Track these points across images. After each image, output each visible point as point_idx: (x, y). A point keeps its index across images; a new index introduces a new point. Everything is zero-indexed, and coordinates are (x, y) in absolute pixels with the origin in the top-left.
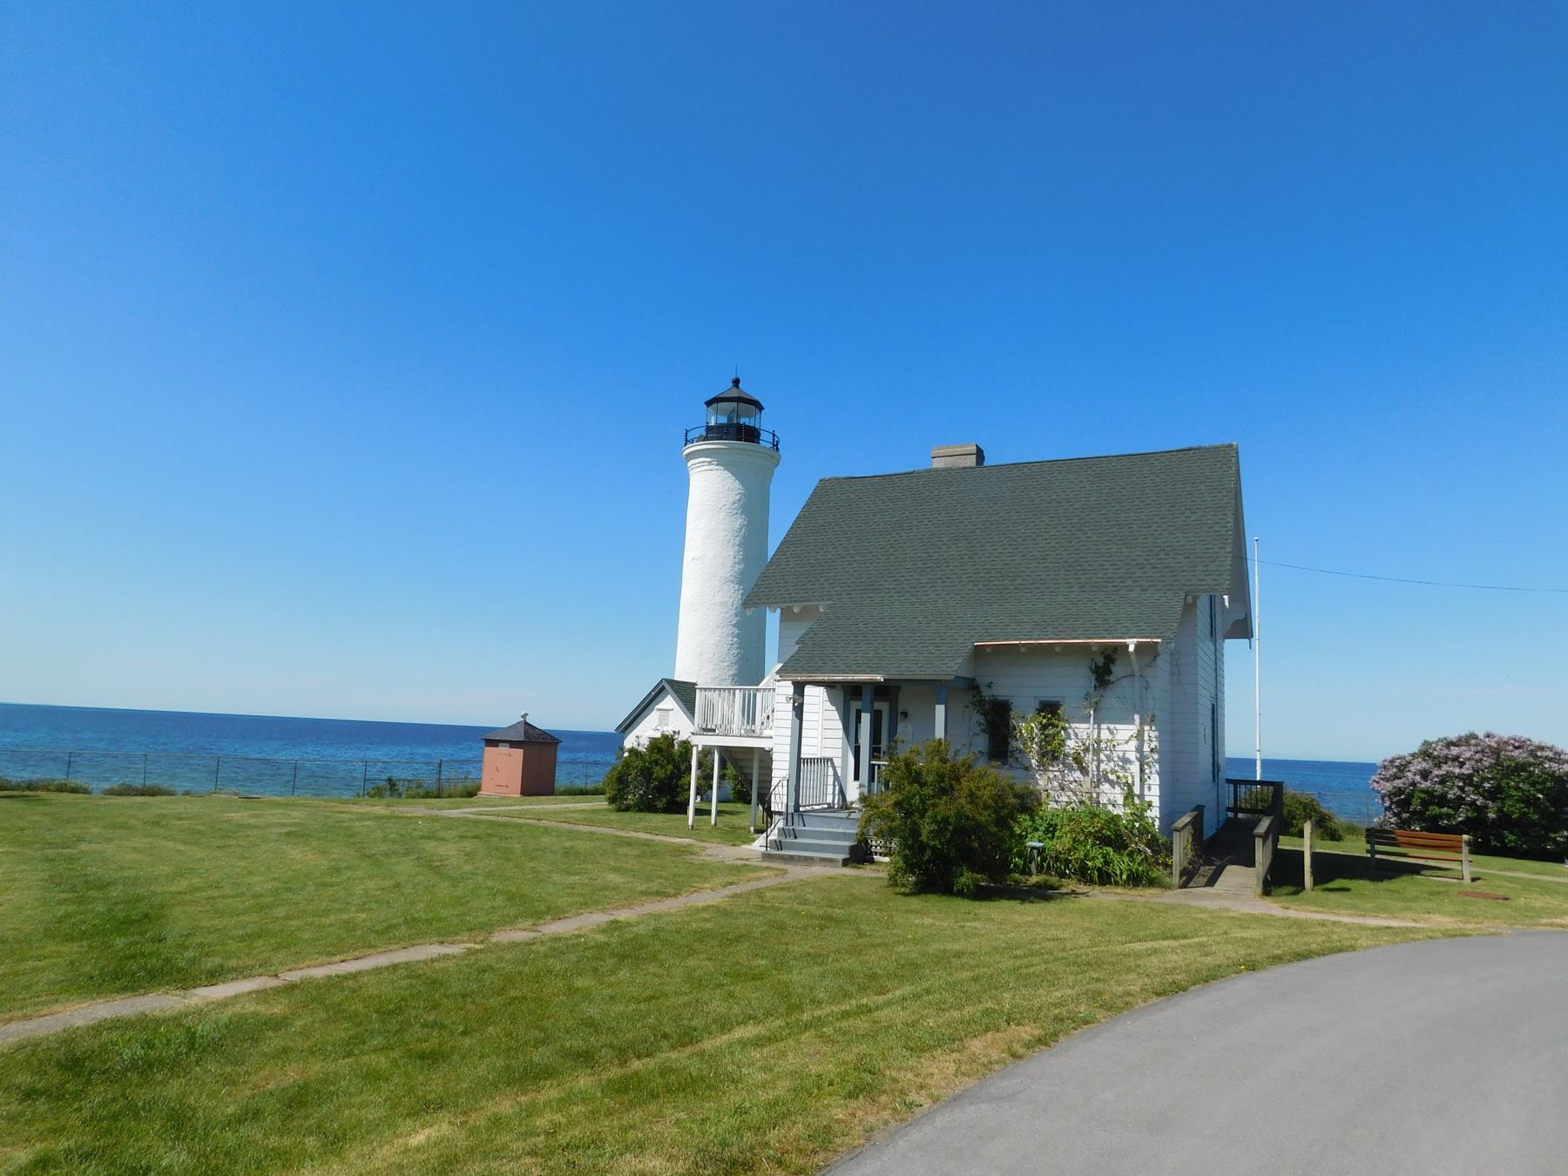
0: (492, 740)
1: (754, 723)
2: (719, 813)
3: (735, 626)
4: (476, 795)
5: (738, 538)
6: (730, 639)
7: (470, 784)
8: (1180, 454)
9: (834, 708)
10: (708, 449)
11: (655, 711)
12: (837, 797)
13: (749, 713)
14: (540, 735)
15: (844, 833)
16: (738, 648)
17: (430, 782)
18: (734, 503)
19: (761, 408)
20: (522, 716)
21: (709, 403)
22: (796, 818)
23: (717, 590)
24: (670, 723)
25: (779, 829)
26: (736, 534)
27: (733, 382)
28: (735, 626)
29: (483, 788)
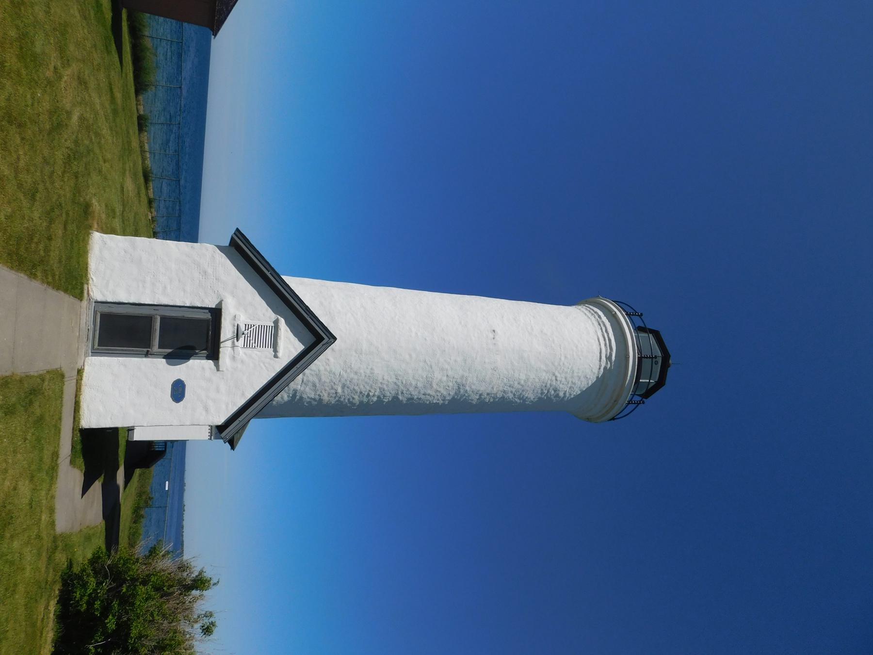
5: (511, 396)
6: (377, 394)
11: (274, 316)
18: (555, 391)
23: (450, 373)
24: (249, 351)
26: (518, 394)
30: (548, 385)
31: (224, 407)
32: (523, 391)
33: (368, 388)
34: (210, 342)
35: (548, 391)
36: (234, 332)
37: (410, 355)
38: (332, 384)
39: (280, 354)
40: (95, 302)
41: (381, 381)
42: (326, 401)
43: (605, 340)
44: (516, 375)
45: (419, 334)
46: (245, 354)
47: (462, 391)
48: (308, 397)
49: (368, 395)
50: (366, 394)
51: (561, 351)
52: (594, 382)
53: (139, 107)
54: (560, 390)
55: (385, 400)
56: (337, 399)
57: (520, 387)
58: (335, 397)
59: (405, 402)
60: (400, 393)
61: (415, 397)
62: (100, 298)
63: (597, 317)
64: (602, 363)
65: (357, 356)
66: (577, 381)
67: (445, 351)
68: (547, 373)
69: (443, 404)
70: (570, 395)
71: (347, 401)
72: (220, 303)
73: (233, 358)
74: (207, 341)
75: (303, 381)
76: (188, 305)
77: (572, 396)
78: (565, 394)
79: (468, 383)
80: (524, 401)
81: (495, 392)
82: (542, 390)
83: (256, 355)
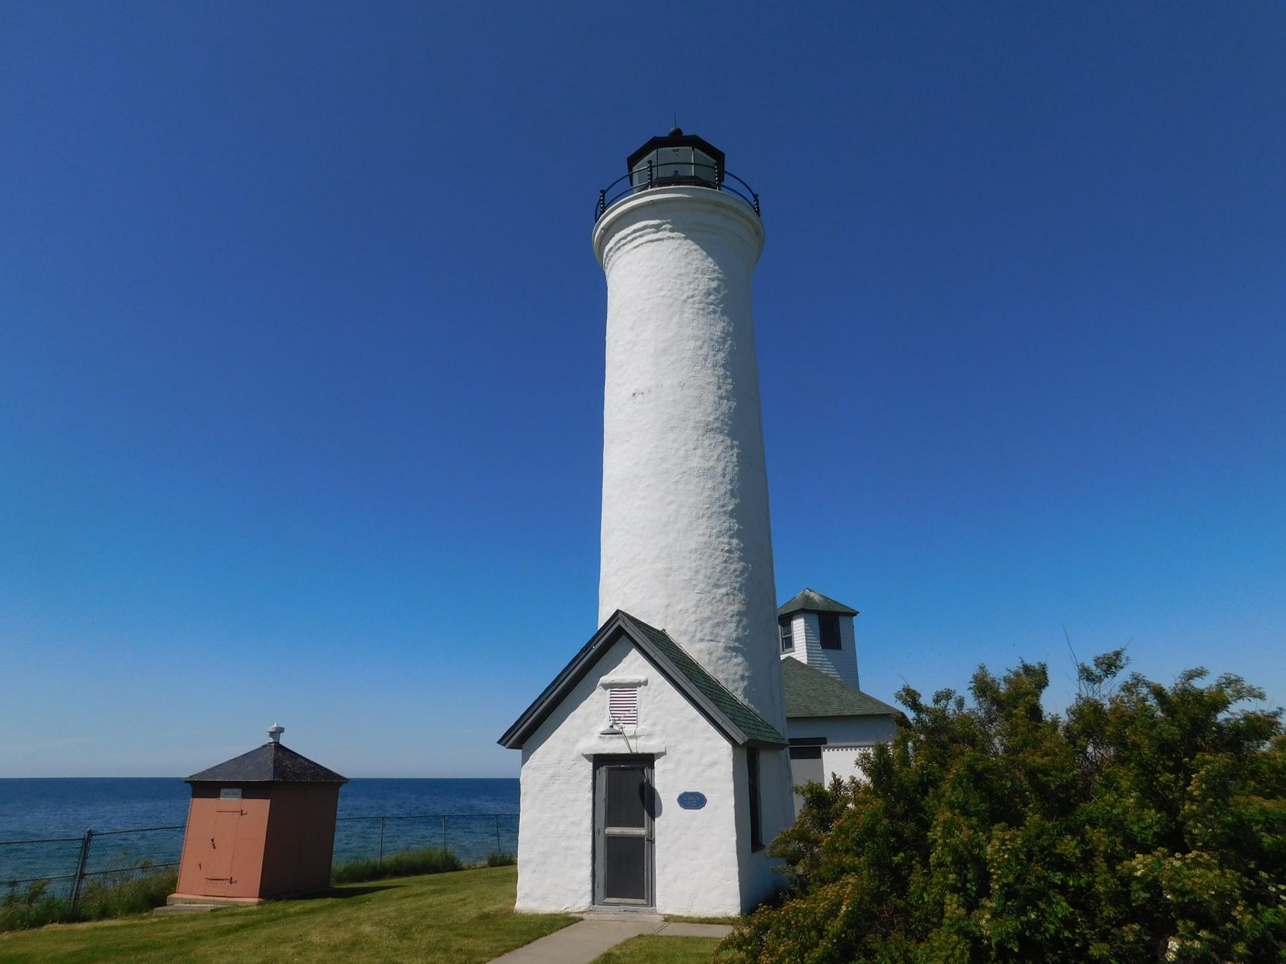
0: (205, 787)
3: (732, 514)
5: (721, 355)
6: (726, 540)
10: (653, 203)
11: (599, 690)
16: (741, 559)
17: (58, 889)
18: (709, 294)
20: (272, 734)
23: (691, 446)
24: (641, 717)
26: (717, 346)
28: (732, 514)
29: (182, 884)
30: (701, 306)
31: (709, 743)
32: (712, 340)
33: (718, 553)
34: (633, 766)
35: (711, 304)
36: (619, 738)
37: (670, 503)
38: (715, 601)
39: (642, 678)
40: (594, 904)
41: (707, 538)
42: (741, 606)
43: (635, 238)
44: (689, 354)
45: (643, 495)
46: (644, 721)
47: (716, 425)
48: (736, 631)
49: (729, 551)
50: (728, 554)
51: (653, 298)
52: (692, 242)
53: (478, 866)
54: (707, 287)
55: (736, 528)
56: (736, 592)
57: (706, 345)
58: (734, 595)
60: (723, 509)
61: (729, 487)
62: (588, 899)
63: (611, 253)
64: (665, 237)
65: (673, 574)
66: (694, 266)
67: (661, 458)
68: (684, 312)
69: (738, 447)
70: (714, 271)
71: (739, 579)
72: (587, 756)
73: (649, 735)
74: (633, 769)
75: (712, 640)
76: (591, 795)
77: (717, 268)
78: (713, 280)
79: (704, 419)
80: (728, 334)
81: (716, 379)
82: (709, 313)
83: (645, 707)
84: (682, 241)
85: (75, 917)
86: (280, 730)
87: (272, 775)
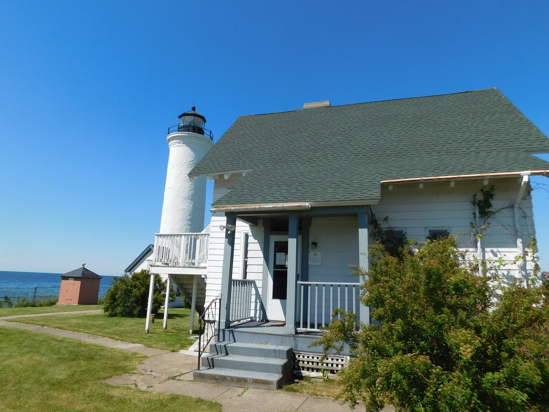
0: (65, 277)
1: (194, 258)
2: (170, 316)
3: (189, 220)
4: (55, 304)
6: (186, 226)
7: (52, 299)
8: (460, 95)
9: (257, 241)
10: (179, 136)
12: (258, 312)
13: (191, 252)
14: (91, 274)
15: (275, 351)
17: (30, 300)
18: (191, 162)
19: (205, 121)
20: (82, 265)
21: (180, 117)
22: (227, 333)
25: (211, 345)
27: (192, 108)
28: (189, 220)
29: (59, 300)
33: (184, 229)
59: (191, 216)
84: (185, 147)
85: (34, 306)
86: (85, 264)
87: (81, 275)
